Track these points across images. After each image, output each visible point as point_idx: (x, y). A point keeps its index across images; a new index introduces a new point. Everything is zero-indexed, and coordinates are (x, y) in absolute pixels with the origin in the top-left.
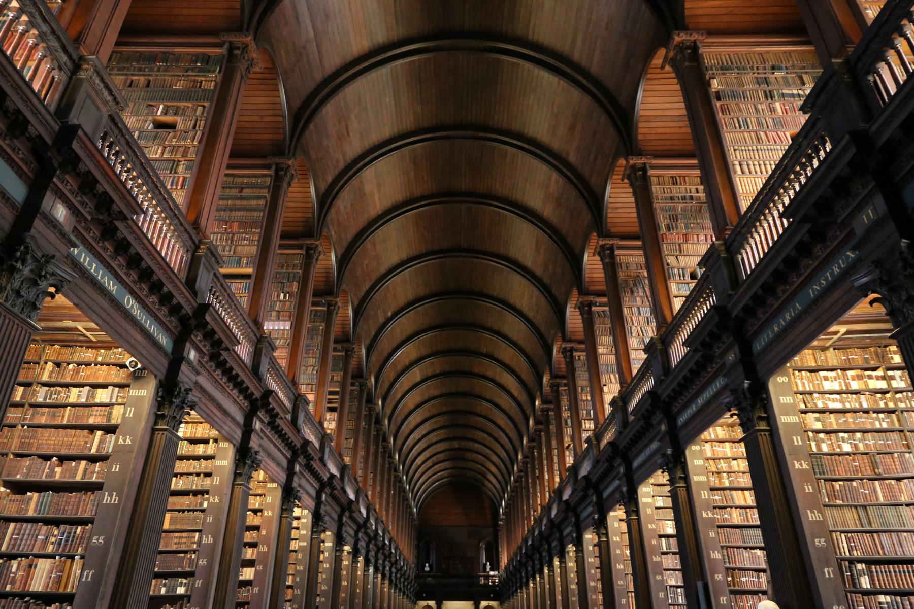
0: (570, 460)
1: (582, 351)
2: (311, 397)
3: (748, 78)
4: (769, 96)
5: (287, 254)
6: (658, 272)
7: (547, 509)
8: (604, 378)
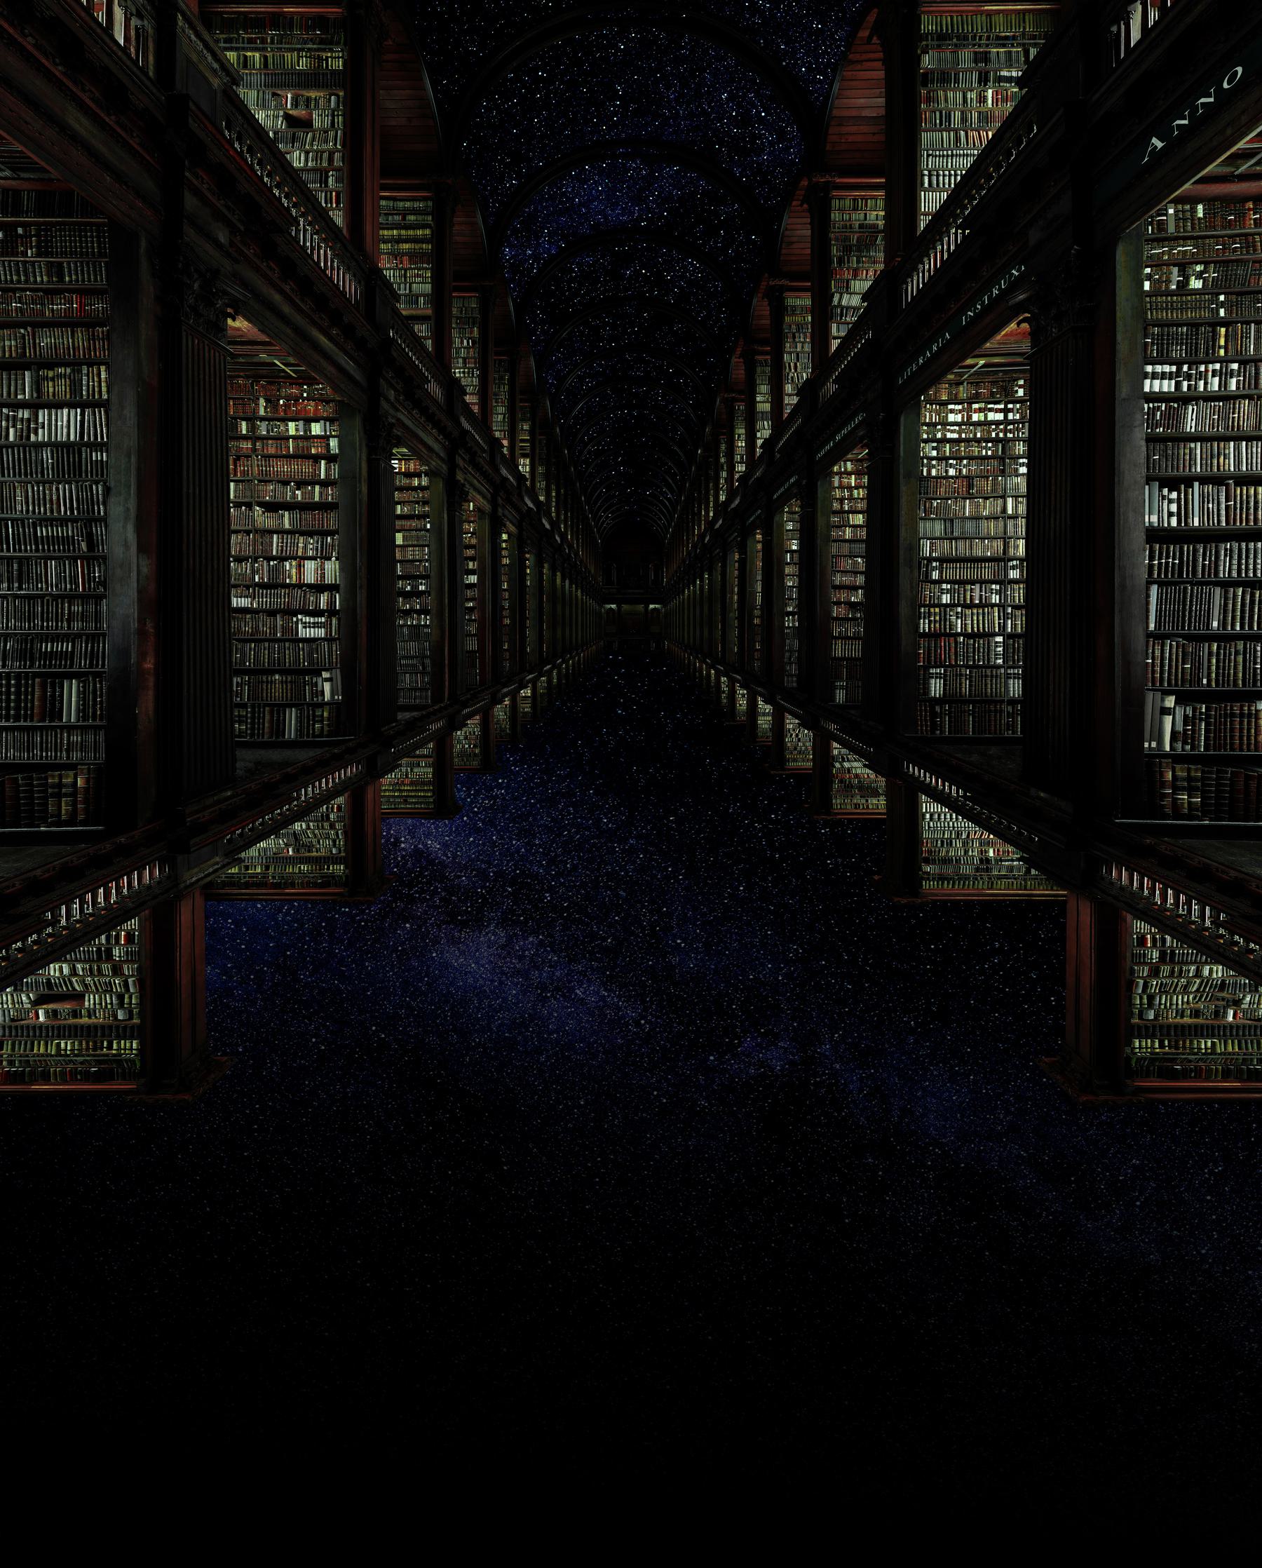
0: (722, 498)
1: (742, 401)
2: (505, 443)
3: (966, 55)
4: (984, 80)
5: (464, 298)
6: (823, 312)
7: (702, 536)
8: (759, 424)
